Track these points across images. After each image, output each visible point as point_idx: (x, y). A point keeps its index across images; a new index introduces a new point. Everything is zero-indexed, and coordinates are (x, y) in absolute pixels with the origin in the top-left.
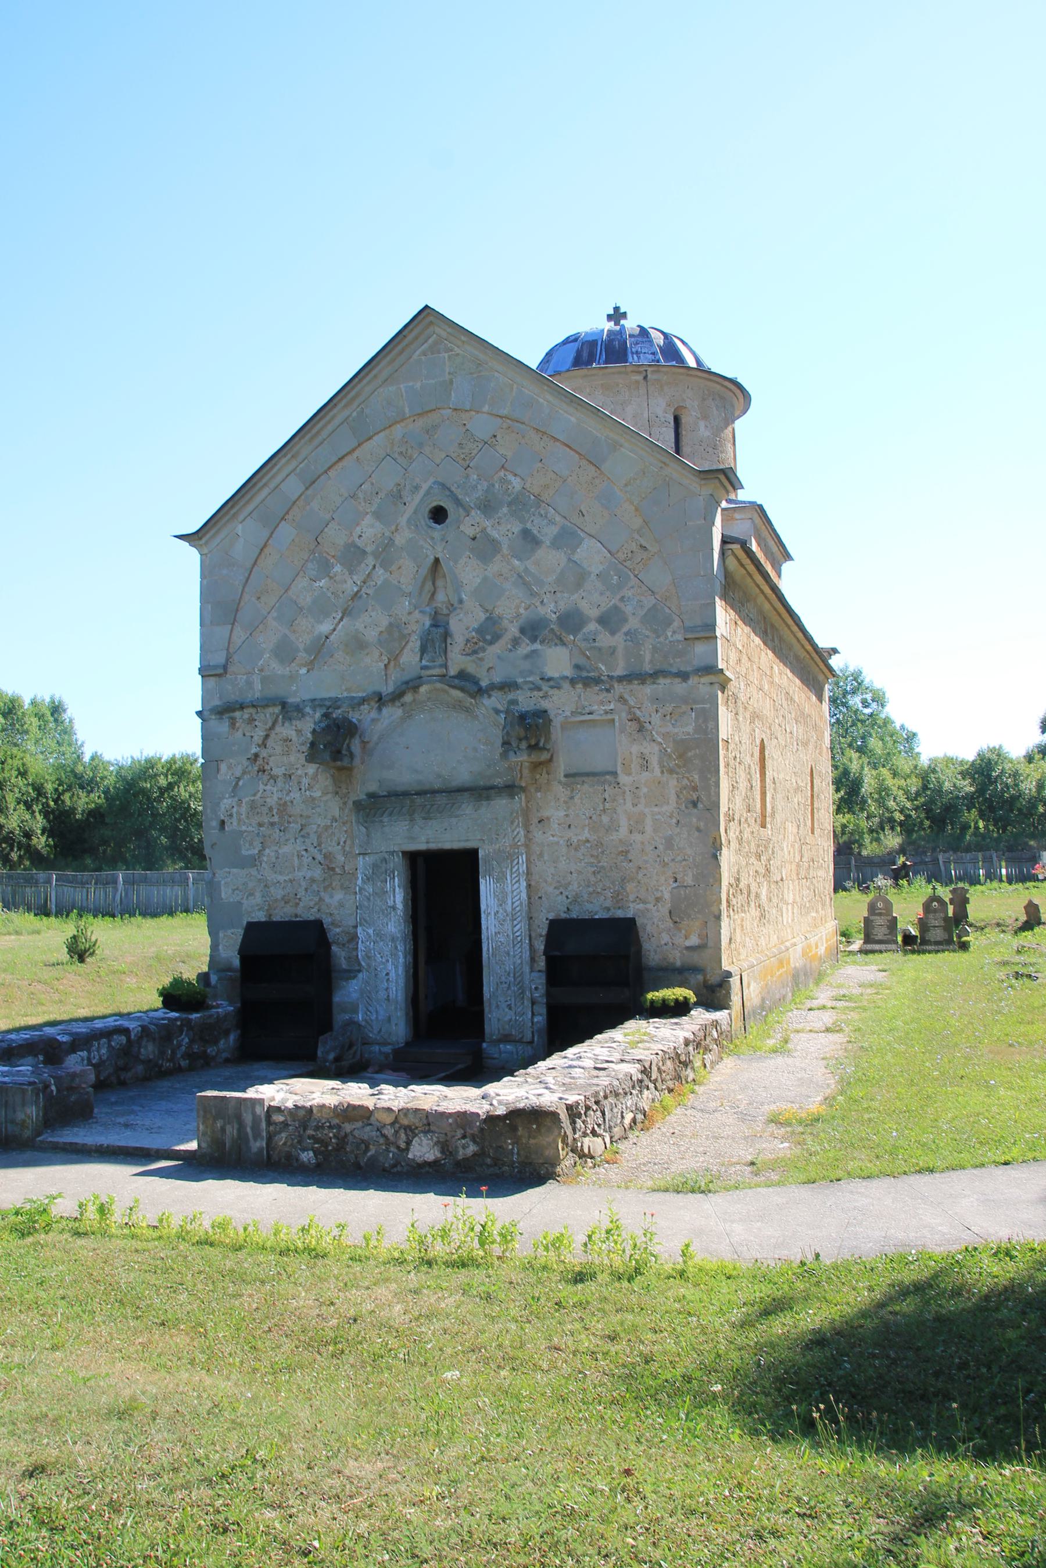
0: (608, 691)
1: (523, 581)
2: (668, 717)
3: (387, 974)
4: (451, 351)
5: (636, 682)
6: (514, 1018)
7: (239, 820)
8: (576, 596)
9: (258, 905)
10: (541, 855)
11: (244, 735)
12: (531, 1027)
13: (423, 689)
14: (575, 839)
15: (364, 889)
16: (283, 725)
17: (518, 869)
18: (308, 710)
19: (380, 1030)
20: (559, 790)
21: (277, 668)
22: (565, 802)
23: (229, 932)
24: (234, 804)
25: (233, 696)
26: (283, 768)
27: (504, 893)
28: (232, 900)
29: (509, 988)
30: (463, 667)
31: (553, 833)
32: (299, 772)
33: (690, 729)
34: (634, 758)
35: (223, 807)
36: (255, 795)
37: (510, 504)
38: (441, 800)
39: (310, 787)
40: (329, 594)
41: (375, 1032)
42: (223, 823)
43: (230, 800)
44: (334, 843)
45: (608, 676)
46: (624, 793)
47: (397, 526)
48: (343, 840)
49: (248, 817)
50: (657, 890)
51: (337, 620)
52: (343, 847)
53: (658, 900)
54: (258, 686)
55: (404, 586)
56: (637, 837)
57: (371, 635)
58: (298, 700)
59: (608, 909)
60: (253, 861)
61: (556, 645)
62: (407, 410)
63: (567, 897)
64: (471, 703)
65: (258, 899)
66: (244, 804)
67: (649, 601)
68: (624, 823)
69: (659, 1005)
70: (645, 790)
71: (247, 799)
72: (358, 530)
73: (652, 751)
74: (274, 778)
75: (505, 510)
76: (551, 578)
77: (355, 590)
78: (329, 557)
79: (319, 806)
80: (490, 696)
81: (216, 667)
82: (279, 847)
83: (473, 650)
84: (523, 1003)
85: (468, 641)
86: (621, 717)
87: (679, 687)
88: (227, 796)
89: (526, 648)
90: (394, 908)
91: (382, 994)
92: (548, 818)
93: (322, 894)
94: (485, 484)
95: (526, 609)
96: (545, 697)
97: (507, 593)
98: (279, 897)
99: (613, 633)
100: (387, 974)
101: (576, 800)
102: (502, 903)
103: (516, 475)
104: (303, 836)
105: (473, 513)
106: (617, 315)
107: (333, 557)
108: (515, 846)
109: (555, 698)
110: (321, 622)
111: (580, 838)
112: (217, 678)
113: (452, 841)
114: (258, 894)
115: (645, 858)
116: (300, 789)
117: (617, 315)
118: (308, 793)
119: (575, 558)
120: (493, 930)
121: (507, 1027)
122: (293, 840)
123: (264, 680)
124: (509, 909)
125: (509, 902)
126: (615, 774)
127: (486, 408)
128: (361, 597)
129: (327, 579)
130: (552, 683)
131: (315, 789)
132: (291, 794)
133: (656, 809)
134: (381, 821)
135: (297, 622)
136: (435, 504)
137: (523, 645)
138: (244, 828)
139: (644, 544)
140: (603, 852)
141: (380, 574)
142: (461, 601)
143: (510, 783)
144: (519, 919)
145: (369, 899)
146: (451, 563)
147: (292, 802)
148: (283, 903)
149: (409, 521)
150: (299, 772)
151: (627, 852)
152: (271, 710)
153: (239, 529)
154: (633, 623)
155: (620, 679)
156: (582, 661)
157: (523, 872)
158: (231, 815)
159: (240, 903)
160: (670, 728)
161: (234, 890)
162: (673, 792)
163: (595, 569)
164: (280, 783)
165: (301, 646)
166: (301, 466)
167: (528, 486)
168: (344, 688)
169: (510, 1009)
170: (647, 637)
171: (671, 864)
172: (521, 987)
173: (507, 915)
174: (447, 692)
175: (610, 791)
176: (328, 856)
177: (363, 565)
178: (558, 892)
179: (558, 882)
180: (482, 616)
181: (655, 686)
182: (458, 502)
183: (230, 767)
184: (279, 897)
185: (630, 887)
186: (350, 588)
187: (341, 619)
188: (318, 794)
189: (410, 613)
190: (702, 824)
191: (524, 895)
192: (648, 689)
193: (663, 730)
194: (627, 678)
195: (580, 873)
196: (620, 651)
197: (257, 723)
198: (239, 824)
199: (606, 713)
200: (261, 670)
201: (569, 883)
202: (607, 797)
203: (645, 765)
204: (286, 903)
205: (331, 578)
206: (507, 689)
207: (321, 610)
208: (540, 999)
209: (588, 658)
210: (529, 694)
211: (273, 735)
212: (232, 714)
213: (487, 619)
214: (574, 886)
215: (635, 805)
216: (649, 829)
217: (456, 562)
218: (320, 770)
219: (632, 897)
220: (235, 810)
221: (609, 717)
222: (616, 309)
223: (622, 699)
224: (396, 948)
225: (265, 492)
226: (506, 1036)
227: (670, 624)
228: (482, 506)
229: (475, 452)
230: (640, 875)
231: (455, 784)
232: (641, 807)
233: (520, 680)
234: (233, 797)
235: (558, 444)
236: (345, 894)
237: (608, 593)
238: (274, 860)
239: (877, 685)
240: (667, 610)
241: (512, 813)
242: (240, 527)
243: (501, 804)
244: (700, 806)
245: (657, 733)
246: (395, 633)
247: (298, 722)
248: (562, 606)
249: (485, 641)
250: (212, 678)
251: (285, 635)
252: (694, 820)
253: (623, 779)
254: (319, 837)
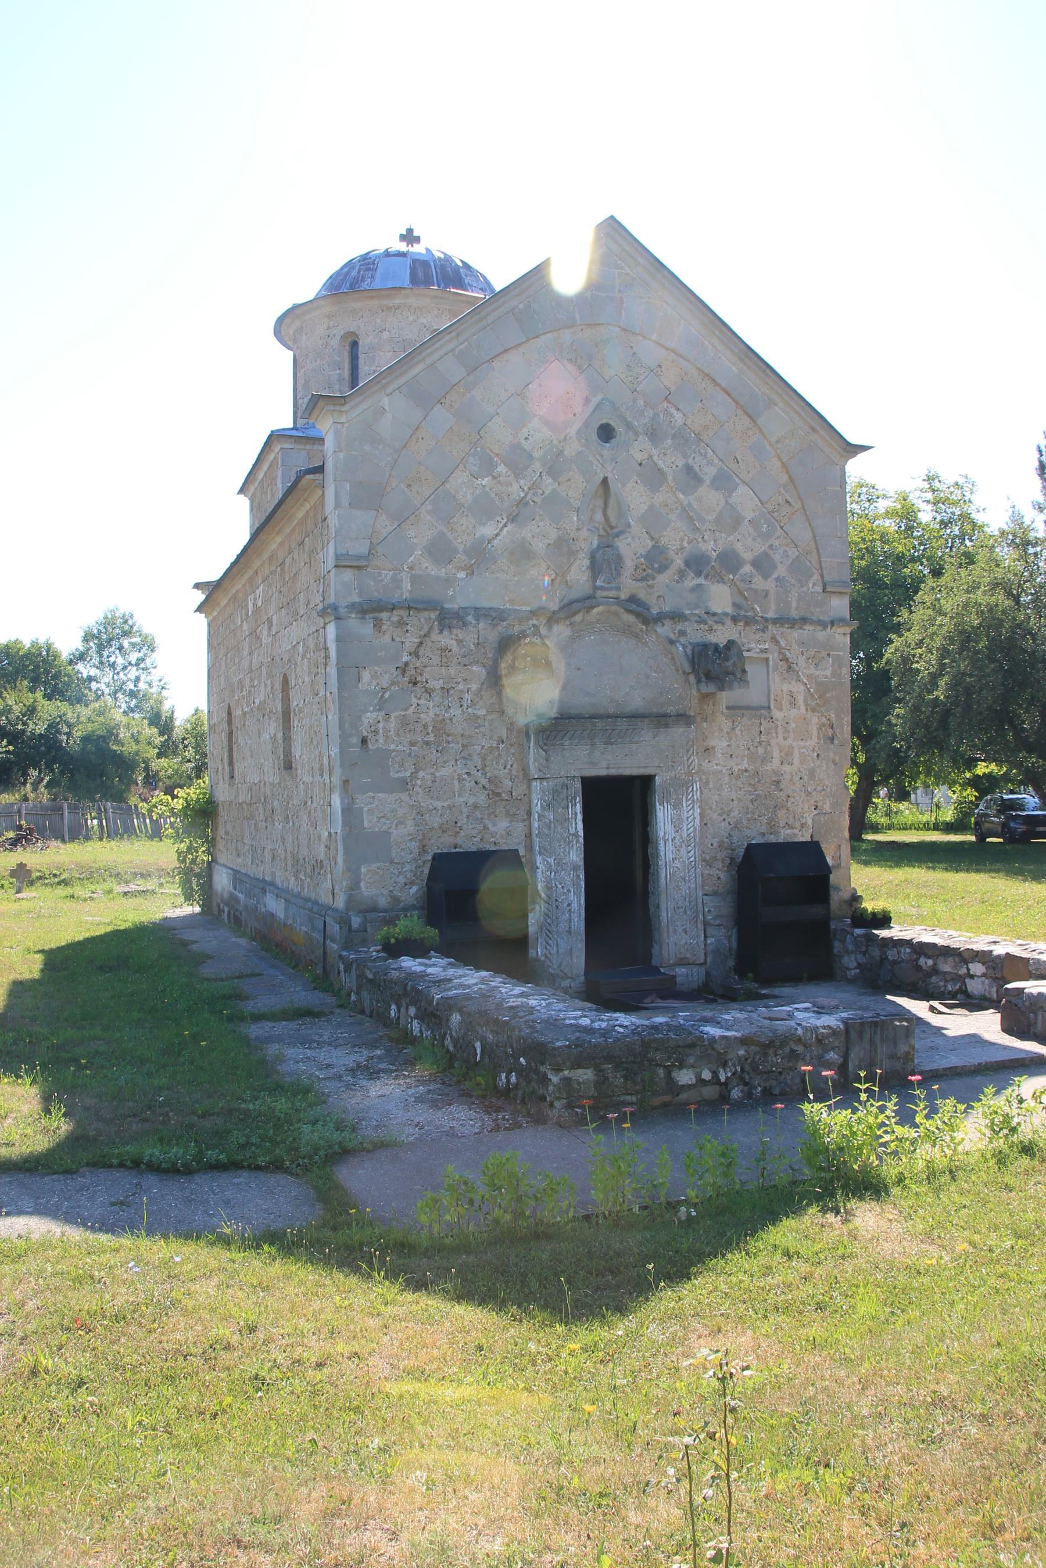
0: (763, 631)
1: (688, 516)
2: (810, 661)
3: (569, 905)
4: (622, 268)
5: (787, 626)
7: (387, 737)
8: (731, 538)
9: (410, 835)
10: (707, 783)
11: (393, 640)
12: (705, 949)
13: (595, 611)
14: (736, 769)
15: (544, 816)
16: (441, 632)
18: (470, 618)
19: (561, 964)
20: (723, 722)
21: (429, 567)
22: (728, 733)
23: (374, 866)
24: (380, 718)
25: (376, 594)
26: (441, 681)
27: (680, 818)
28: (377, 830)
29: (685, 912)
30: (634, 592)
32: (461, 687)
33: (828, 673)
34: (785, 695)
35: (366, 721)
36: (406, 710)
37: (674, 437)
38: (622, 725)
39: (473, 704)
40: (493, 495)
41: (555, 967)
42: (364, 741)
43: (375, 714)
44: (501, 767)
45: (762, 617)
46: (777, 726)
47: (565, 436)
48: (510, 763)
49: (398, 735)
50: (803, 817)
51: (501, 525)
52: (510, 770)
53: (803, 825)
54: (407, 586)
55: (572, 500)
56: (787, 768)
57: (539, 546)
58: (456, 606)
59: (763, 834)
60: (405, 785)
61: (718, 582)
62: (578, 317)
63: (729, 824)
64: (641, 630)
65: (410, 827)
66: (392, 720)
67: (793, 553)
68: (776, 754)
69: (869, 919)
70: (793, 725)
71: (396, 714)
72: (525, 430)
73: (799, 689)
74: (429, 692)
75: (669, 441)
76: (712, 517)
77: (522, 495)
78: (492, 455)
79: (484, 726)
80: (663, 625)
81: (359, 557)
82: (436, 769)
83: (644, 577)
84: (697, 926)
85: (637, 567)
86: (773, 657)
87: (821, 635)
88: (371, 708)
89: (691, 581)
90: (576, 835)
91: (564, 926)
92: (713, 748)
93: (486, 822)
94: (651, 413)
95: (689, 543)
96: (711, 630)
97: (673, 524)
98: (436, 825)
99: (766, 577)
100: (569, 905)
101: (737, 731)
102: (678, 829)
103: (678, 409)
104: (464, 758)
105: (641, 438)
106: (409, 237)
107: (497, 455)
108: (689, 773)
109: (719, 633)
110: (484, 524)
111: (740, 767)
112: (356, 572)
113: (631, 767)
114: (410, 823)
115: (793, 787)
116: (461, 706)
117: (409, 237)
118: (470, 710)
119: (732, 501)
120: (670, 856)
121: (683, 950)
122: (453, 762)
123: (414, 579)
124: (685, 835)
125: (685, 828)
126: (769, 708)
127: (654, 337)
128: (527, 503)
129: (490, 478)
130: (716, 618)
131: (477, 707)
132: (451, 711)
133: (802, 743)
134: (562, 745)
135: (455, 519)
136: (604, 421)
137: (689, 578)
138: (393, 747)
139: (789, 499)
140: (759, 781)
141: (548, 484)
142: (629, 526)
143: (681, 712)
145: (550, 827)
146: (620, 485)
147: (451, 720)
148: (440, 832)
149: (578, 432)
150: (461, 687)
151: (778, 782)
152: (426, 614)
153: (386, 401)
154: (781, 571)
155: (775, 621)
156: (739, 600)
158: (376, 732)
159: (387, 833)
160: (812, 670)
161: (379, 818)
162: (815, 728)
163: (749, 515)
164: (437, 697)
165: (461, 548)
166: (461, 347)
167: (689, 422)
168: (507, 599)
169: (686, 933)
170: (794, 585)
171: (813, 794)
174: (617, 614)
175: (765, 725)
176: (493, 780)
177: (530, 470)
178: (722, 819)
179: (722, 809)
180: (650, 544)
181: (801, 631)
182: (629, 426)
183: (374, 676)
184: (436, 825)
185: (781, 814)
186: (516, 491)
187: (505, 526)
188: (483, 712)
189: (578, 529)
190: (837, 758)
191: (697, 821)
192: (796, 634)
193: (807, 672)
194: (779, 621)
195: (740, 800)
196: (772, 596)
197: (409, 628)
198: (386, 741)
199: (762, 651)
200: (411, 568)
201: (731, 810)
202: (762, 729)
203: (793, 704)
204: (443, 831)
205: (494, 478)
206: (677, 620)
207: (484, 510)
208: (712, 921)
209: (745, 598)
210: (696, 626)
211: (428, 642)
212: (377, 615)
213: (654, 547)
214: (735, 813)
215: (785, 739)
216: (796, 760)
217: (624, 485)
218: (484, 686)
219: (782, 823)
220: (381, 725)
221: (765, 655)
222: (410, 231)
223: (774, 640)
224: (578, 876)
225: (421, 366)
226: (681, 959)
227: (812, 576)
228: (649, 434)
229: (642, 377)
230: (790, 803)
231: (629, 709)
232: (790, 741)
233: (687, 612)
234: (379, 710)
235: (718, 388)
236: (511, 821)
237: (759, 540)
238: (429, 783)
239: (146, 630)
240: (808, 564)
241: (688, 742)
242: (386, 399)
243: (678, 732)
244: (836, 742)
245: (803, 673)
246: (563, 547)
247: (459, 631)
248: (721, 546)
249: (653, 569)
250: (348, 570)
251: (441, 533)
252: (832, 754)
253: (776, 714)
254: (484, 759)
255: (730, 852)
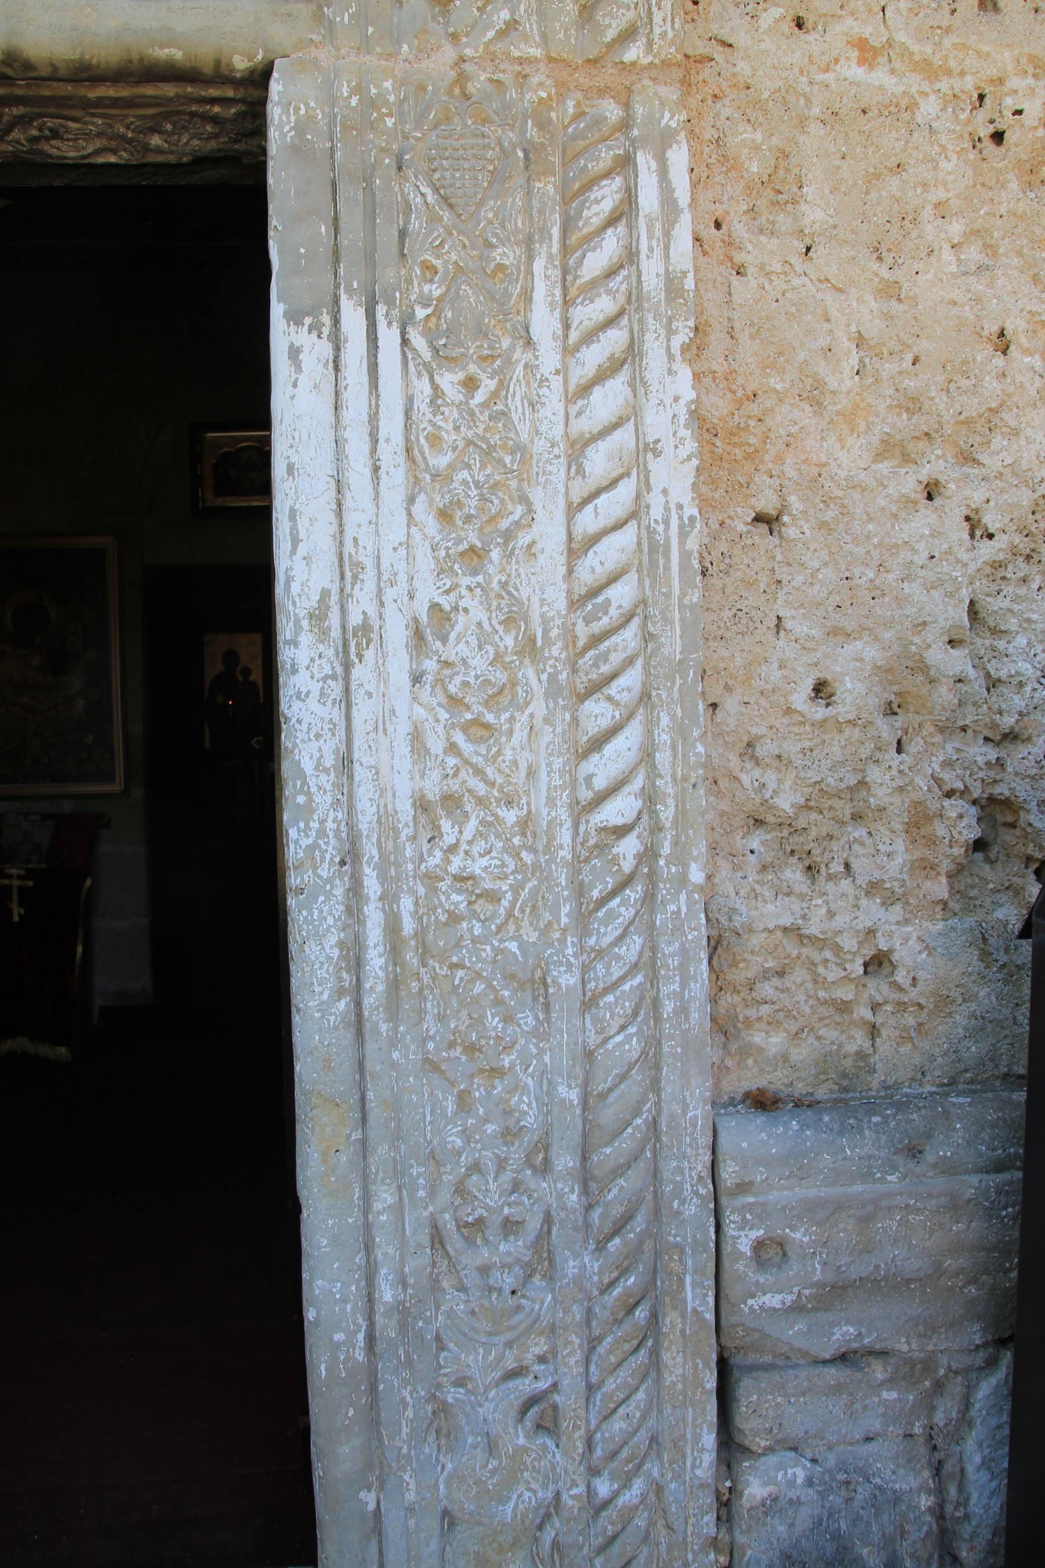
6: (572, 1497)
17: (630, 256)
31: (871, 31)
144: (631, 679)
157: (672, 285)
172: (633, 1254)
173: (529, 649)
178: (910, 483)
179: (912, 405)
255: (981, 753)
